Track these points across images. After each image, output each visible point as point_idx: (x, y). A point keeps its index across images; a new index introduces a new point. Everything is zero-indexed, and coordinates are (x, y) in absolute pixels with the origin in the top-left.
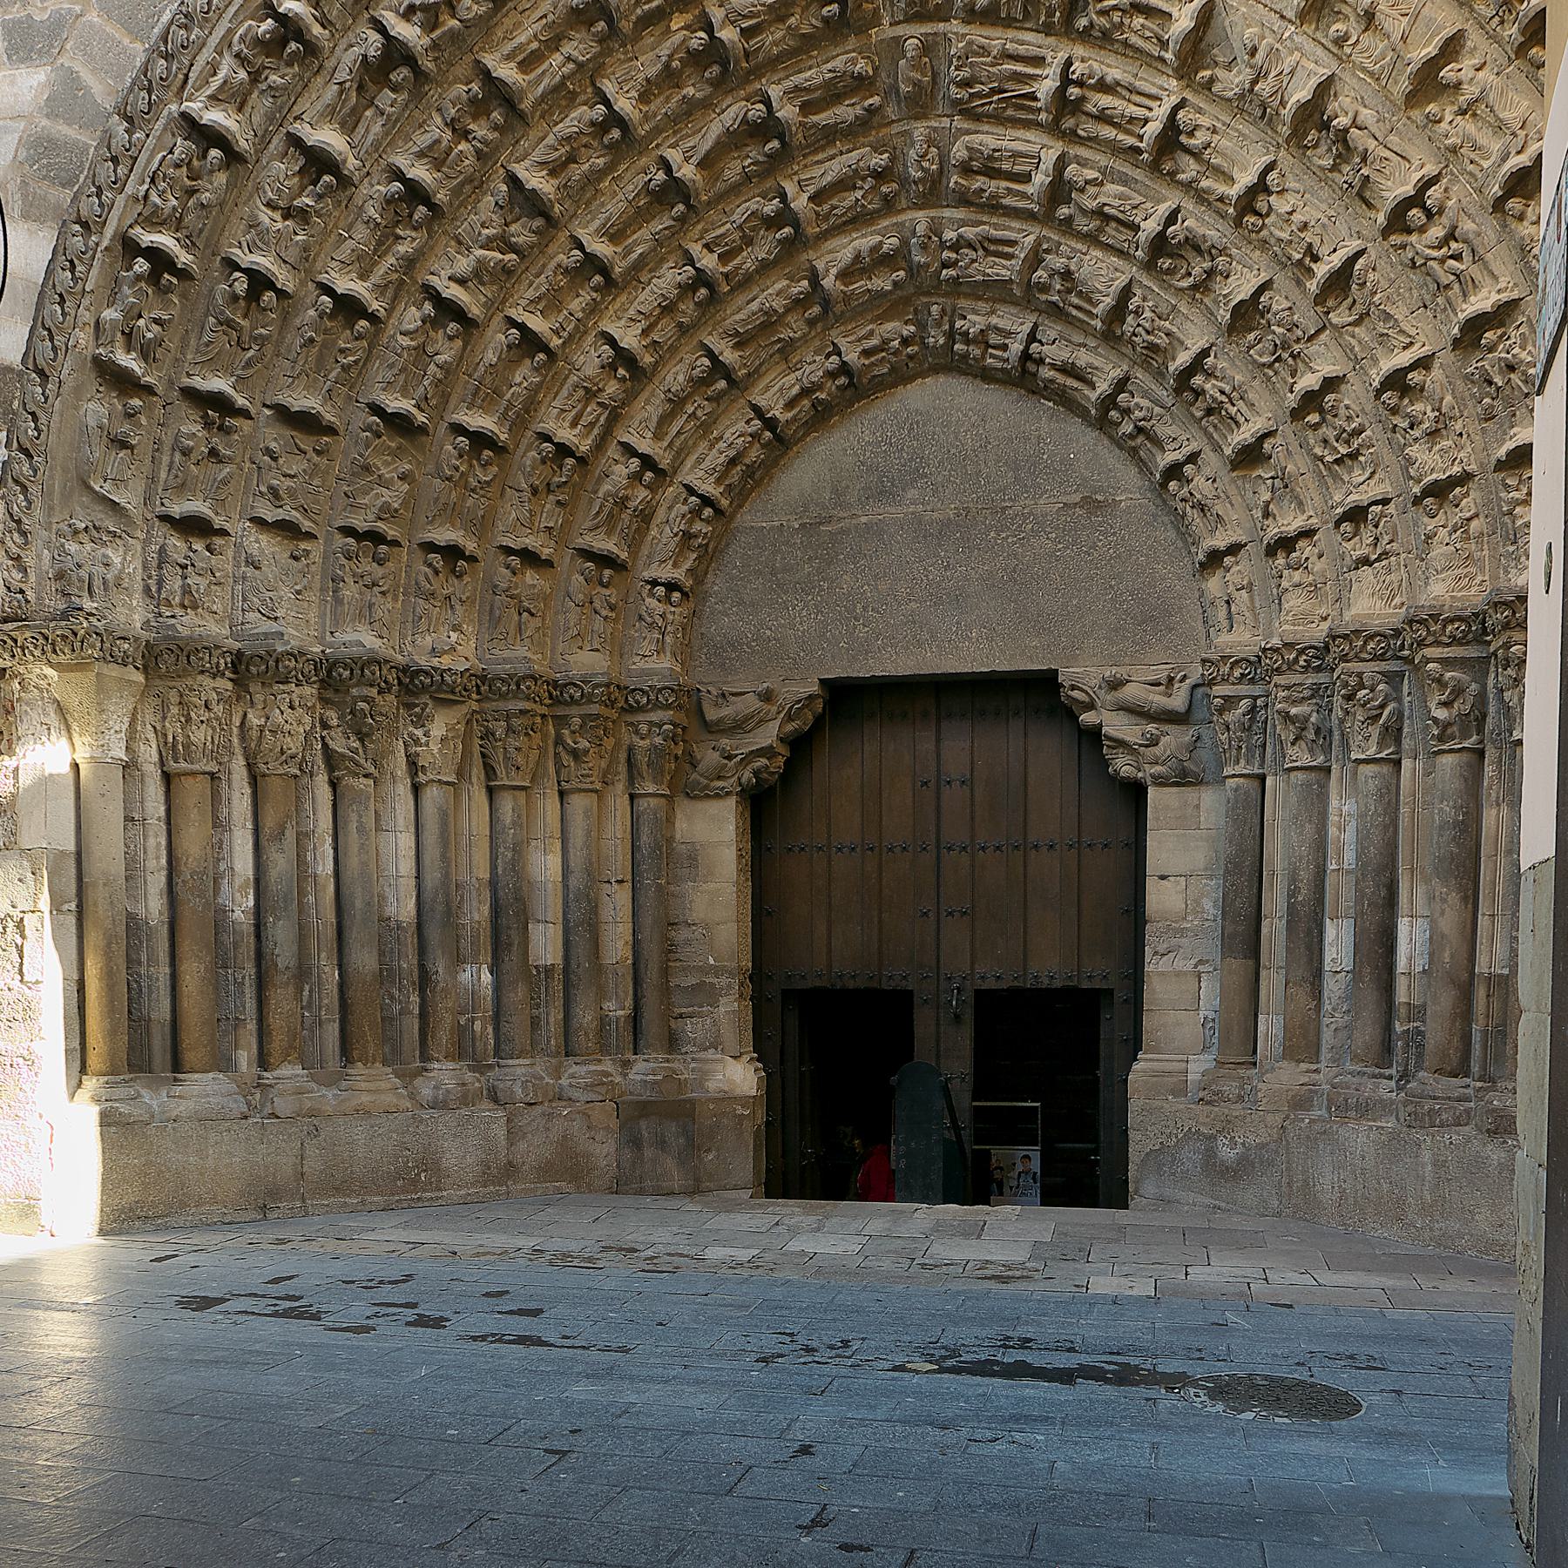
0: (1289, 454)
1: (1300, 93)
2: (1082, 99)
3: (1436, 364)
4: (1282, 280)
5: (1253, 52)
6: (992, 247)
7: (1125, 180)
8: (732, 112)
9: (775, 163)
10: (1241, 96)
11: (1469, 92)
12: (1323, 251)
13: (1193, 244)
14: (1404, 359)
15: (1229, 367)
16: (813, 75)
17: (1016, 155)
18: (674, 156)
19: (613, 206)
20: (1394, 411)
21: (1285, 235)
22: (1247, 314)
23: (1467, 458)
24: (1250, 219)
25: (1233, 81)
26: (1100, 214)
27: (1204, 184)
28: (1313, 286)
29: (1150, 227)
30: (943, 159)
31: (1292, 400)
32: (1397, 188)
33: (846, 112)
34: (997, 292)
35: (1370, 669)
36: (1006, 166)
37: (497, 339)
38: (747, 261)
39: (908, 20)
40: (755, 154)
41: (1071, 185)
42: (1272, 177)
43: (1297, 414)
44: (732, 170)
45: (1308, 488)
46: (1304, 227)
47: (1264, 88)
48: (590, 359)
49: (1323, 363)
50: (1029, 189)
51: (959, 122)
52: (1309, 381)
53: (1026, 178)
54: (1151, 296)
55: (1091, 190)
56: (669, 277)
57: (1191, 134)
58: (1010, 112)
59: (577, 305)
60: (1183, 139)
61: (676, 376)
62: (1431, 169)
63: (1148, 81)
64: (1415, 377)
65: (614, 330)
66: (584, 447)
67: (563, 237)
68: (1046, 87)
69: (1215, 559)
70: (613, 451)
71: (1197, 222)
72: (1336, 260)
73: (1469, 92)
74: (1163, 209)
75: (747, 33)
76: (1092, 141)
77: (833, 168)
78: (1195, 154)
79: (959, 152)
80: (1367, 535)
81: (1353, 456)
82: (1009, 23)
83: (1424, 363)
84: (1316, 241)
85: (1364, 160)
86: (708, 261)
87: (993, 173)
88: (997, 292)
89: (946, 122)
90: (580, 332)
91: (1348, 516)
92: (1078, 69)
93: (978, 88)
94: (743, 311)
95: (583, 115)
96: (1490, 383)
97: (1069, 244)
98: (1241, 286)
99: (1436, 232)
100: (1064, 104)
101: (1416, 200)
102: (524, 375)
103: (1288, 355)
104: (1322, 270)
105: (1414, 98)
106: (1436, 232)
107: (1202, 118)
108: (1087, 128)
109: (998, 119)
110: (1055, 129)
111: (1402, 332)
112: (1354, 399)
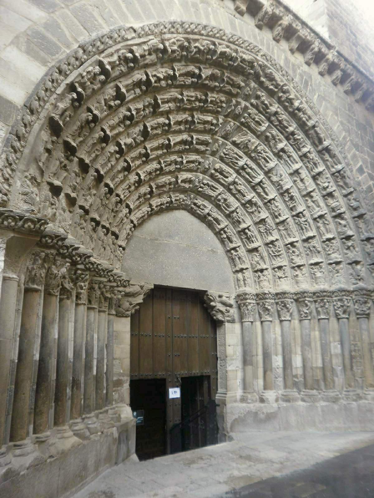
2: (246, 169)
3: (299, 242)
6: (213, 188)
7: (246, 187)
10: (275, 182)
12: (282, 215)
13: (256, 204)
17: (228, 172)
20: (289, 249)
21: (276, 209)
24: (269, 204)
26: (239, 191)
27: (262, 194)
30: (213, 165)
34: (208, 198)
36: (225, 173)
39: (222, 137)
42: (276, 198)
46: (280, 209)
50: (226, 180)
51: (218, 160)
53: (227, 177)
55: (240, 186)
57: (263, 184)
58: (231, 164)
60: (261, 184)
63: (259, 171)
64: (295, 244)
68: (241, 163)
76: (243, 177)
78: (263, 188)
79: (217, 166)
82: (239, 148)
83: (297, 242)
84: (281, 213)
85: (295, 202)
88: (208, 198)
89: (216, 159)
93: (227, 156)
96: (309, 249)
97: (228, 194)
99: (303, 219)
106: (303, 219)
108: (244, 173)
109: (227, 164)
110: (237, 172)
111: (294, 235)
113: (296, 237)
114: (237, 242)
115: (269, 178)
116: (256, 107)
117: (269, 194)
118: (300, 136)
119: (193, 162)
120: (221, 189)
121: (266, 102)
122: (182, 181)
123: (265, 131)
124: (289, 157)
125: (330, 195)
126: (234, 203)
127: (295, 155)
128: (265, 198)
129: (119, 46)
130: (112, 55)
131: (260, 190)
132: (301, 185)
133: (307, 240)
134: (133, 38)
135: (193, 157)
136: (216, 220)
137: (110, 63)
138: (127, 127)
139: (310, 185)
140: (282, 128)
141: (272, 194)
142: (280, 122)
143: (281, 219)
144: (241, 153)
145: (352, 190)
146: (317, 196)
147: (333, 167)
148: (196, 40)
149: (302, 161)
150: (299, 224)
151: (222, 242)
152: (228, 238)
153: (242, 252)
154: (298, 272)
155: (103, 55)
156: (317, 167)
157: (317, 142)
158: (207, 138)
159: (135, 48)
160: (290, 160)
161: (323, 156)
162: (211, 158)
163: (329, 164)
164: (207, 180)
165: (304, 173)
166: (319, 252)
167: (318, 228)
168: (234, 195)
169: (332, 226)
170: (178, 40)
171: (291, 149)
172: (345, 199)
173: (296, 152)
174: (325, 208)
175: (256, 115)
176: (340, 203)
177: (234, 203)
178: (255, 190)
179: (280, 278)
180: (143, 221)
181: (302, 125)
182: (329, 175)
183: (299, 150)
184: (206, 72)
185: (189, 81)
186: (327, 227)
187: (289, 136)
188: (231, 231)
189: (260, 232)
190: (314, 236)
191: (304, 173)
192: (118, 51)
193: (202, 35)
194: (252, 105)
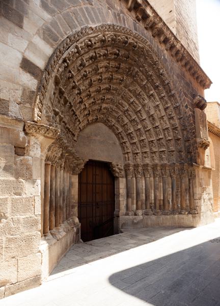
6: (117, 113)
14: (153, 139)
26: (129, 115)
53: (124, 107)
63: (140, 105)
110: (129, 105)
113: (154, 138)
114: (126, 139)
115: (144, 108)
116: (142, 72)
118: (161, 88)
123: (145, 85)
124: (154, 98)
125: (172, 118)
126: (126, 121)
127: (157, 98)
129: (85, 38)
130: (82, 43)
134: (91, 33)
137: (81, 47)
138: (84, 81)
139: (163, 113)
140: (153, 83)
141: (145, 116)
142: (152, 80)
143: (148, 129)
144: (132, 95)
146: (165, 118)
148: (119, 36)
149: (160, 100)
150: (156, 132)
151: (119, 139)
152: (122, 137)
153: (128, 144)
155: (78, 42)
157: (168, 91)
159: (92, 39)
165: (161, 107)
166: (164, 145)
167: (165, 134)
168: (126, 116)
169: (171, 133)
170: (111, 35)
171: (156, 95)
178: (137, 114)
179: (145, 157)
180: (84, 127)
181: (163, 82)
183: (160, 95)
184: (122, 52)
185: (113, 57)
187: (156, 88)
189: (137, 134)
190: (163, 138)
191: (161, 107)
192: (84, 41)
193: (122, 33)
194: (140, 70)
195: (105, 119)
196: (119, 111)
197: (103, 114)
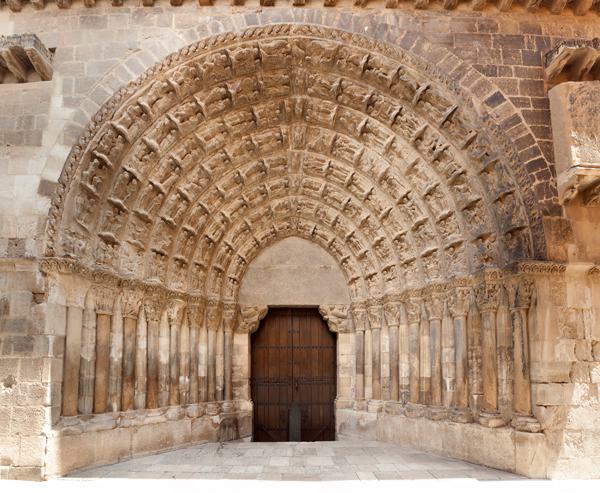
0: (372, 256)
1: (382, 170)
4: (373, 216)
5: (372, 161)
8: (255, 163)
9: (262, 179)
11: (420, 171)
15: (359, 236)
16: (273, 158)
18: (241, 171)
19: (225, 181)
22: (365, 223)
23: (415, 254)
25: (366, 168)
27: (358, 192)
28: (380, 216)
29: (345, 202)
31: (373, 243)
32: (402, 192)
33: (281, 168)
35: (394, 304)
37: (195, 210)
38: (255, 201)
40: (259, 174)
41: (328, 192)
43: (374, 246)
44: (254, 178)
45: (376, 263)
47: (374, 169)
48: (218, 219)
49: (381, 234)
52: (378, 238)
54: (343, 219)
56: (237, 202)
59: (216, 204)
61: (238, 227)
62: (409, 189)
65: (224, 212)
66: (216, 240)
67: (213, 187)
68: (325, 167)
69: (353, 280)
70: (222, 243)
71: (356, 202)
72: (387, 209)
73: (420, 171)
74: (348, 198)
75: (260, 144)
77: (276, 182)
78: (356, 185)
79: (304, 181)
80: (390, 273)
81: (387, 256)
83: (404, 234)
86: (247, 199)
87: (311, 188)
90: (215, 212)
91: (385, 270)
92: (332, 163)
94: (254, 213)
95: (219, 155)
98: (363, 216)
99: (409, 203)
100: (329, 172)
101: (406, 196)
102: (202, 219)
103: (373, 232)
104: (383, 212)
105: (408, 173)
107: (359, 177)
108: (332, 178)
112: (388, 243)
117: (364, 189)
118: (383, 99)
119: (276, 187)
120: (317, 203)
121: (323, 81)
122: (276, 209)
127: (383, 129)
128: (361, 196)
131: (354, 188)
132: (397, 161)
133: (417, 227)
135: (276, 182)
136: (323, 236)
139: (411, 155)
140: (355, 102)
141: (367, 185)
145: (474, 133)
146: (422, 167)
147: (439, 116)
149: (395, 130)
150: (405, 212)
152: (338, 251)
154: (409, 270)
156: (414, 129)
157: (408, 95)
158: (280, 156)
160: (379, 138)
161: (419, 109)
162: (295, 176)
163: (431, 114)
164: (300, 199)
172: (465, 152)
173: (385, 123)
174: (436, 177)
175: (320, 103)
176: (459, 159)
177: (333, 214)
182: (435, 131)
186: (442, 201)
188: (340, 244)
190: (426, 220)
195: (294, 227)
196: (313, 202)
197: (286, 219)
